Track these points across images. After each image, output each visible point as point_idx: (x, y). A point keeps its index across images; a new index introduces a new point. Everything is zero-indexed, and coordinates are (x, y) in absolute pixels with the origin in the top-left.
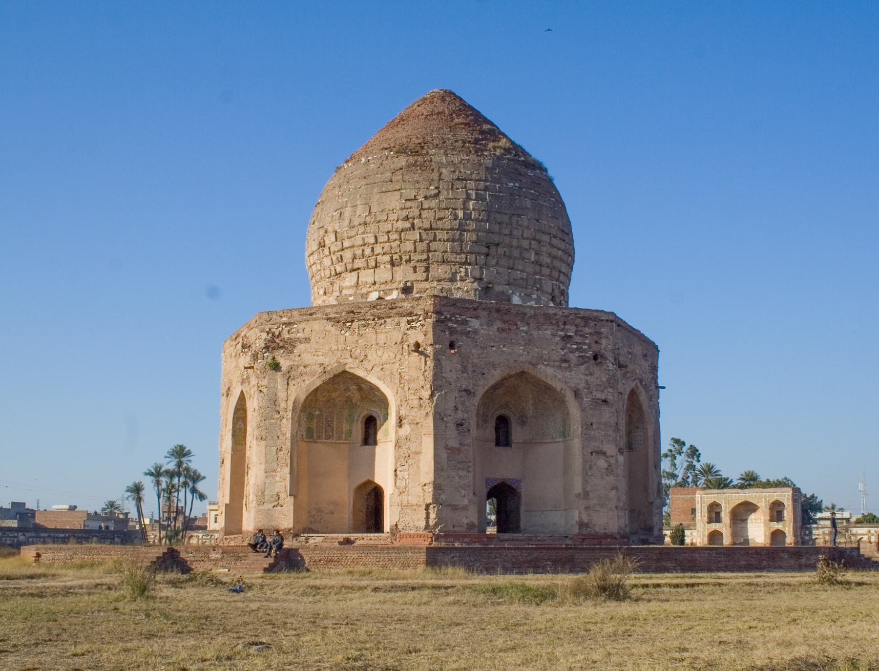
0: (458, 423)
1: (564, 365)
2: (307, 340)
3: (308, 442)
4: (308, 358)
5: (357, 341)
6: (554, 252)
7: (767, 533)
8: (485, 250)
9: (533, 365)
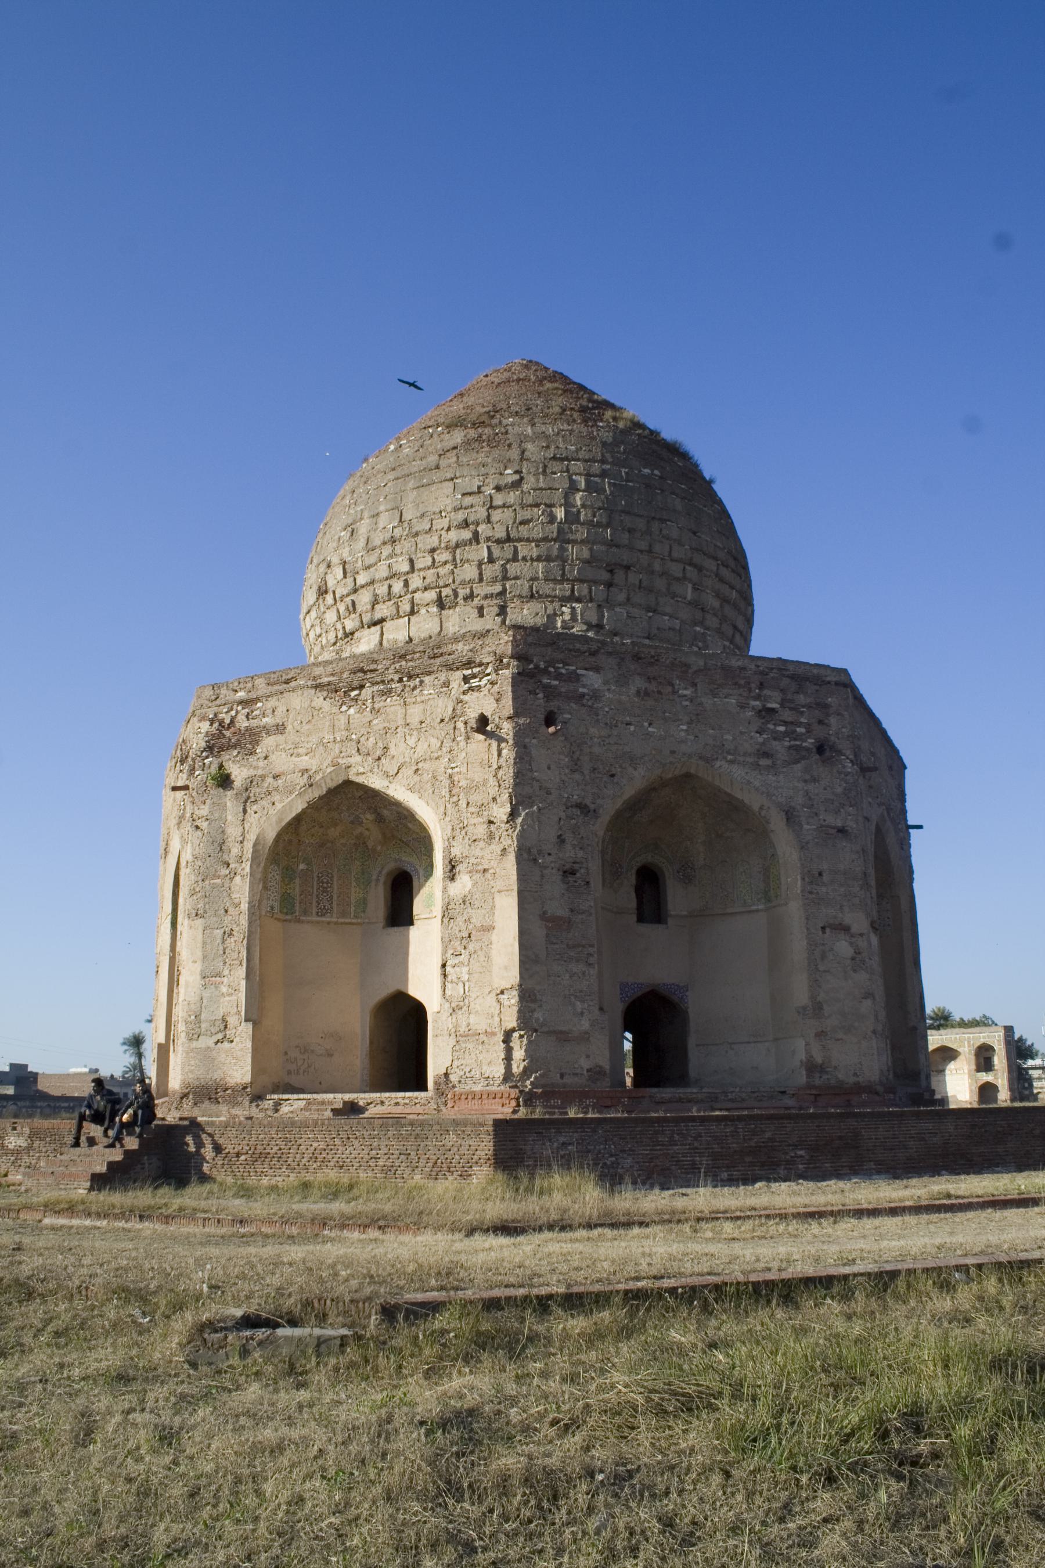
0: (567, 867)
1: (764, 762)
2: (280, 729)
3: (285, 920)
4: (281, 762)
5: (370, 722)
6: (725, 590)
7: (973, 1088)
8: (605, 576)
9: (708, 760)
